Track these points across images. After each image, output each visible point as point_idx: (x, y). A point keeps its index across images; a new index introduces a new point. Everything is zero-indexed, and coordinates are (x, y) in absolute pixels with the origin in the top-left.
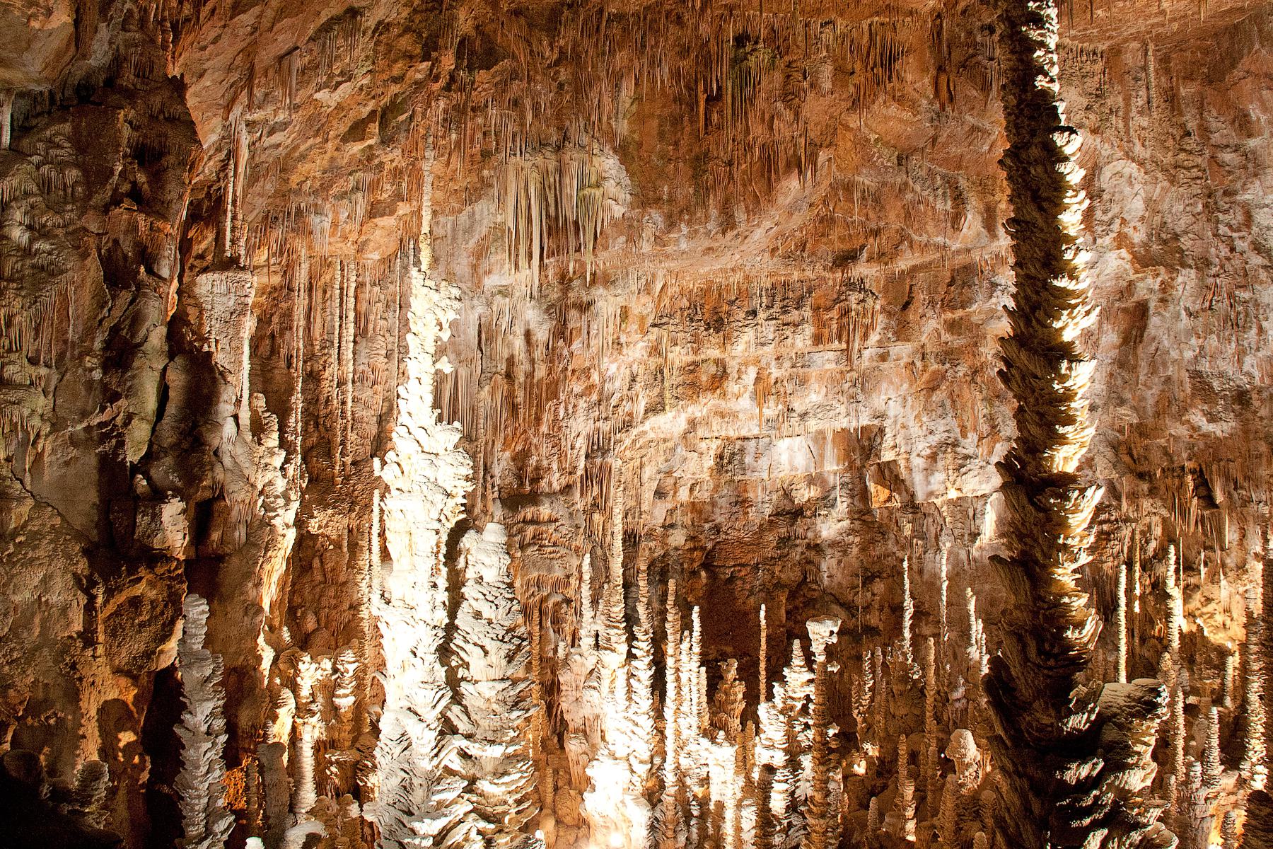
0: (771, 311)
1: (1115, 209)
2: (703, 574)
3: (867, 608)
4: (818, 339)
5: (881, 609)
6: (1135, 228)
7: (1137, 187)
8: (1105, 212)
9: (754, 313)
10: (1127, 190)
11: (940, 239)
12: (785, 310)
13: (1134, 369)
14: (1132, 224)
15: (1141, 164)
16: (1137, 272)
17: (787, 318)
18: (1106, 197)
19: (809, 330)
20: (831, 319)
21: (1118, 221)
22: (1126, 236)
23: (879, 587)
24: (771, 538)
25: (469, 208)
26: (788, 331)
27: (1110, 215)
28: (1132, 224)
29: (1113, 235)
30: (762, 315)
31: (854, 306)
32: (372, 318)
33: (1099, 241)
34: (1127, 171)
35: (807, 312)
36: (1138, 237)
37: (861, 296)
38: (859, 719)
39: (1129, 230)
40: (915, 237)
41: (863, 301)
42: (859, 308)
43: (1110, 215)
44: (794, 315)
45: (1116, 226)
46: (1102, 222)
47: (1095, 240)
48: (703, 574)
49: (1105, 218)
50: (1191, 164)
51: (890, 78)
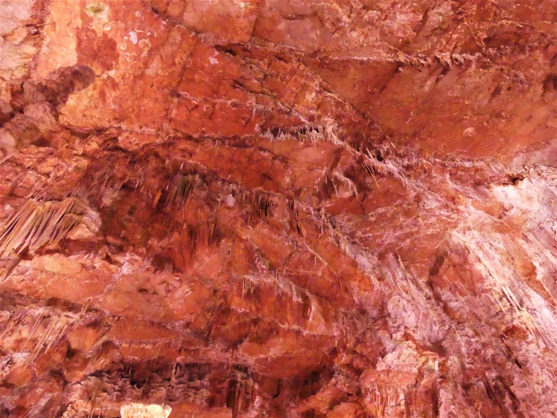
0: (181, 379)
1: (399, 322)
6: (414, 331)
8: (394, 323)
10: (404, 314)
11: (296, 327)
12: (191, 379)
16: (422, 355)
17: (192, 384)
18: (392, 316)
19: (205, 393)
20: (223, 388)
21: (402, 328)
22: (409, 335)
28: (412, 329)
31: (239, 380)
33: (394, 336)
35: (206, 382)
37: (245, 375)
39: (410, 332)
41: (246, 378)
42: (243, 381)
44: (197, 383)
45: (402, 328)
47: (391, 337)
49: (396, 325)
51: (266, 214)
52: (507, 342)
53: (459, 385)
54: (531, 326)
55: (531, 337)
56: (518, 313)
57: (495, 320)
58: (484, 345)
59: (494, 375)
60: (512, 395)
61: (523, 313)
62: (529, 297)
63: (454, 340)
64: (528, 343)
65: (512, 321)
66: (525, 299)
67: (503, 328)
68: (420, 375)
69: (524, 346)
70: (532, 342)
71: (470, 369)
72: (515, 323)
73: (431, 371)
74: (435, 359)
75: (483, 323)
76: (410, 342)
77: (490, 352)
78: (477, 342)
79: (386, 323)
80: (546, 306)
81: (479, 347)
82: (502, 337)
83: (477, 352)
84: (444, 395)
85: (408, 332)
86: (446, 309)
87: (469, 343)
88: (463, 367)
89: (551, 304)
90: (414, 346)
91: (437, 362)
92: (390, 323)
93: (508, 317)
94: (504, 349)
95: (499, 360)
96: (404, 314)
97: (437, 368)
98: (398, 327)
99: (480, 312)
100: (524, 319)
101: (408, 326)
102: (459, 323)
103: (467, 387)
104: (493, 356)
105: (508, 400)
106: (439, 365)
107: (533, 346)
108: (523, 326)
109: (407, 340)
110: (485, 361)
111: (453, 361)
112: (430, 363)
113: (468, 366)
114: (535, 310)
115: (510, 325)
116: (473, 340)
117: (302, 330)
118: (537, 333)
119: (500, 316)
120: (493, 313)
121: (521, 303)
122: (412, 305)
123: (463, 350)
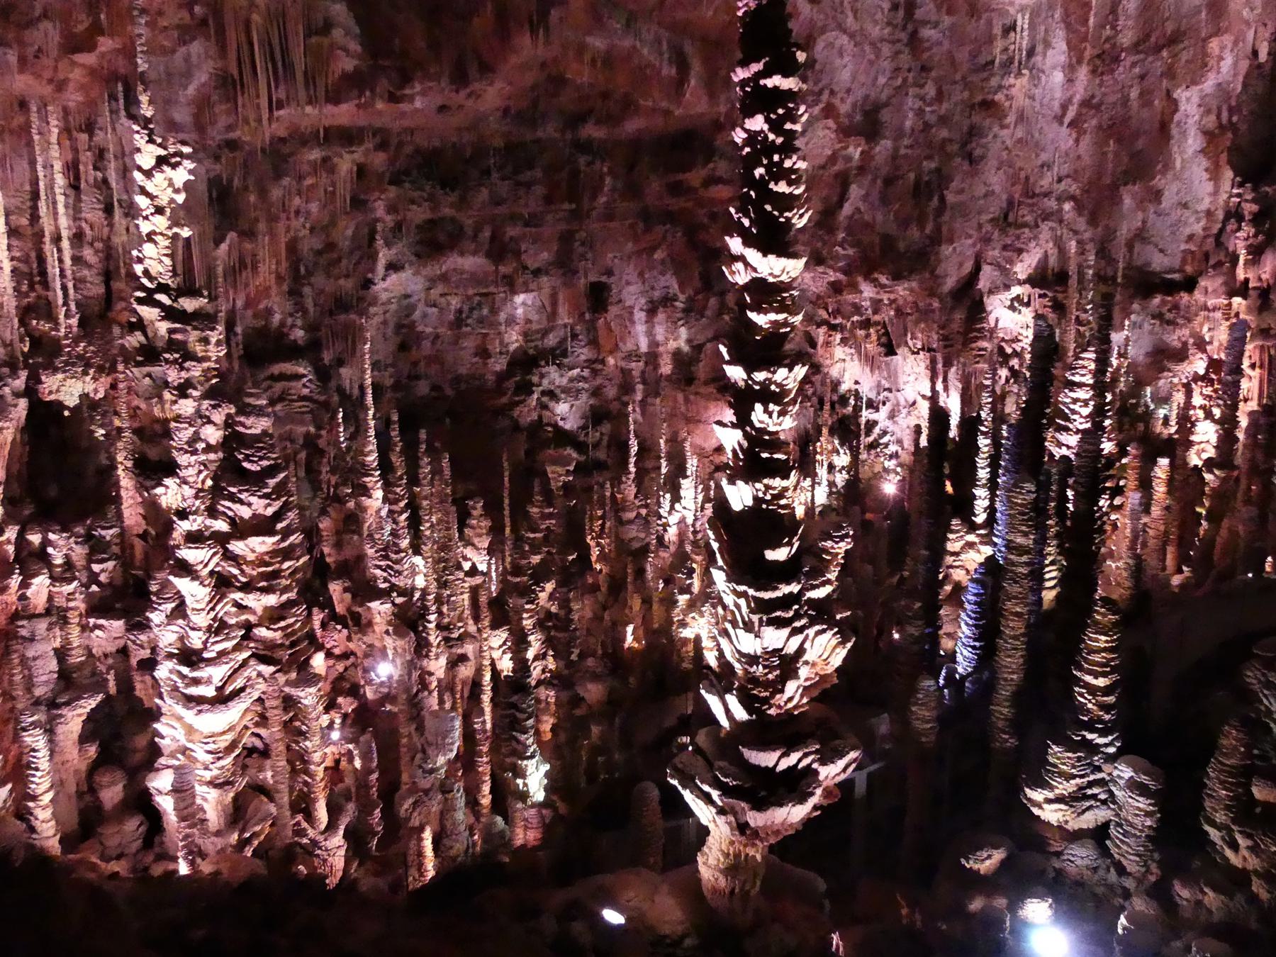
2: (448, 420)
3: (596, 446)
4: (549, 200)
5: (609, 446)
7: (846, 59)
9: (487, 172)
11: (664, 104)
13: (831, 231)
14: (839, 96)
15: (852, 36)
18: (817, 67)
19: (539, 190)
23: (606, 428)
24: (510, 384)
25: (183, 50)
26: (522, 192)
27: (820, 85)
29: (821, 106)
30: (495, 175)
31: (583, 168)
32: (81, 167)
34: (838, 43)
35: (538, 173)
36: (844, 108)
37: (590, 158)
38: (592, 543)
39: (836, 102)
40: (641, 102)
43: (820, 85)
44: (527, 176)
45: (825, 97)
48: (448, 420)
52: (976, 119)
53: (879, 181)
54: (1020, 101)
55: (1011, 119)
56: (1012, 81)
57: (974, 78)
58: (944, 120)
59: (933, 165)
60: (942, 199)
61: (1018, 82)
62: (1047, 45)
63: (899, 109)
64: (1003, 127)
65: (995, 93)
66: (1039, 48)
67: (979, 98)
68: (833, 159)
69: (996, 129)
70: (1007, 127)
71: (906, 156)
72: (999, 97)
73: (849, 159)
74: (859, 145)
75: (958, 77)
76: (831, 123)
77: (944, 133)
78: (932, 112)
80: (1063, 67)
81: (932, 119)
82: (972, 107)
83: (927, 126)
84: (855, 191)
85: (834, 101)
86: (914, 41)
87: (920, 113)
88: (895, 156)
89: (1074, 60)
90: (834, 126)
91: (860, 149)
93: (994, 82)
94: (965, 129)
95: (949, 148)
96: (838, 62)
97: (857, 156)
98: (820, 92)
99: (962, 55)
100: (1014, 91)
101: (836, 89)
102: (924, 69)
103: (888, 182)
104: (944, 141)
105: (935, 201)
106: (862, 153)
107: (1005, 132)
108: (1007, 104)
109: (827, 118)
110: (930, 145)
111: (884, 146)
112: (851, 149)
113: (903, 151)
114: (1043, 72)
115: (990, 97)
116: (928, 109)
117: (672, 108)
118: (1021, 118)
119: (985, 74)
120: (982, 60)
121: (1031, 53)
123: (908, 124)
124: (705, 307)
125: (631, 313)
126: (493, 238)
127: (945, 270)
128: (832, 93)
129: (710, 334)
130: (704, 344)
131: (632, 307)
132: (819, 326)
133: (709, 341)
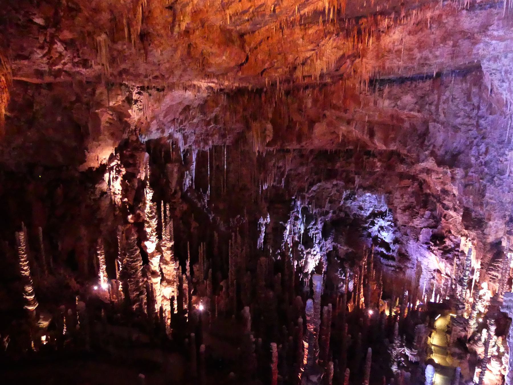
1: (432, 141)
2: (348, 227)
7: (441, 133)
8: (429, 141)
15: (443, 124)
21: (432, 146)
27: (430, 143)
39: (436, 150)
43: (430, 143)
45: (431, 148)
46: (426, 145)
48: (348, 227)
49: (428, 144)
50: (470, 123)
78: (483, 158)
79: (425, 139)
85: (435, 150)
92: (426, 142)
98: (429, 146)
122: (444, 128)
124: (424, 214)
125: (396, 209)
126: (347, 176)
127: (489, 232)
128: (434, 146)
129: (426, 224)
130: (421, 228)
131: (396, 207)
132: (462, 236)
133: (425, 227)
